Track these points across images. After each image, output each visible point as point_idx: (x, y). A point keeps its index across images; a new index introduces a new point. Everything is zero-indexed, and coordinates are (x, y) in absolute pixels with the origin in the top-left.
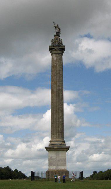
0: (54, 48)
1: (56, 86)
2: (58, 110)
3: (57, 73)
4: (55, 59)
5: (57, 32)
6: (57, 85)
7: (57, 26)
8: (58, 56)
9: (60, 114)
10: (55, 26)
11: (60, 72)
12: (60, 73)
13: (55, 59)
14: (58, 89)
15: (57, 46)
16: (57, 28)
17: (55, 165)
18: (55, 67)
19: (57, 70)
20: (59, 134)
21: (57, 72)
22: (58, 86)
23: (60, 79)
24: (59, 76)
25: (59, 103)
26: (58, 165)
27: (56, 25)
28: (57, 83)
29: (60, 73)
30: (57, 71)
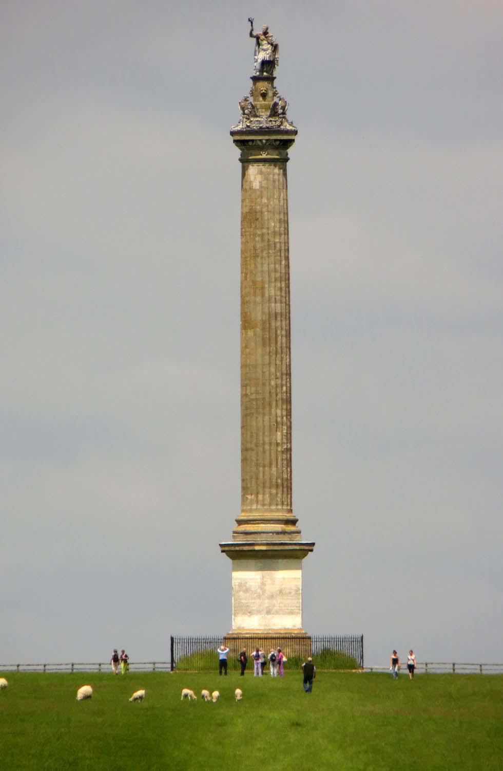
0: (253, 141)
1: (259, 299)
2: (267, 400)
3: (266, 244)
4: (256, 185)
5: (264, 63)
6: (263, 295)
7: (265, 33)
8: (269, 174)
9: (279, 412)
10: (254, 33)
11: (277, 240)
12: (275, 243)
13: (256, 185)
14: (266, 310)
15: (262, 131)
16: (265, 45)
17: (259, 612)
18: (257, 219)
19: (265, 231)
20: (274, 491)
21: (262, 240)
22: (270, 297)
23: (275, 271)
24: (272, 258)
25: (273, 370)
26: (269, 612)
27: (258, 31)
28: (263, 288)
29: (278, 246)
30: (266, 237)
